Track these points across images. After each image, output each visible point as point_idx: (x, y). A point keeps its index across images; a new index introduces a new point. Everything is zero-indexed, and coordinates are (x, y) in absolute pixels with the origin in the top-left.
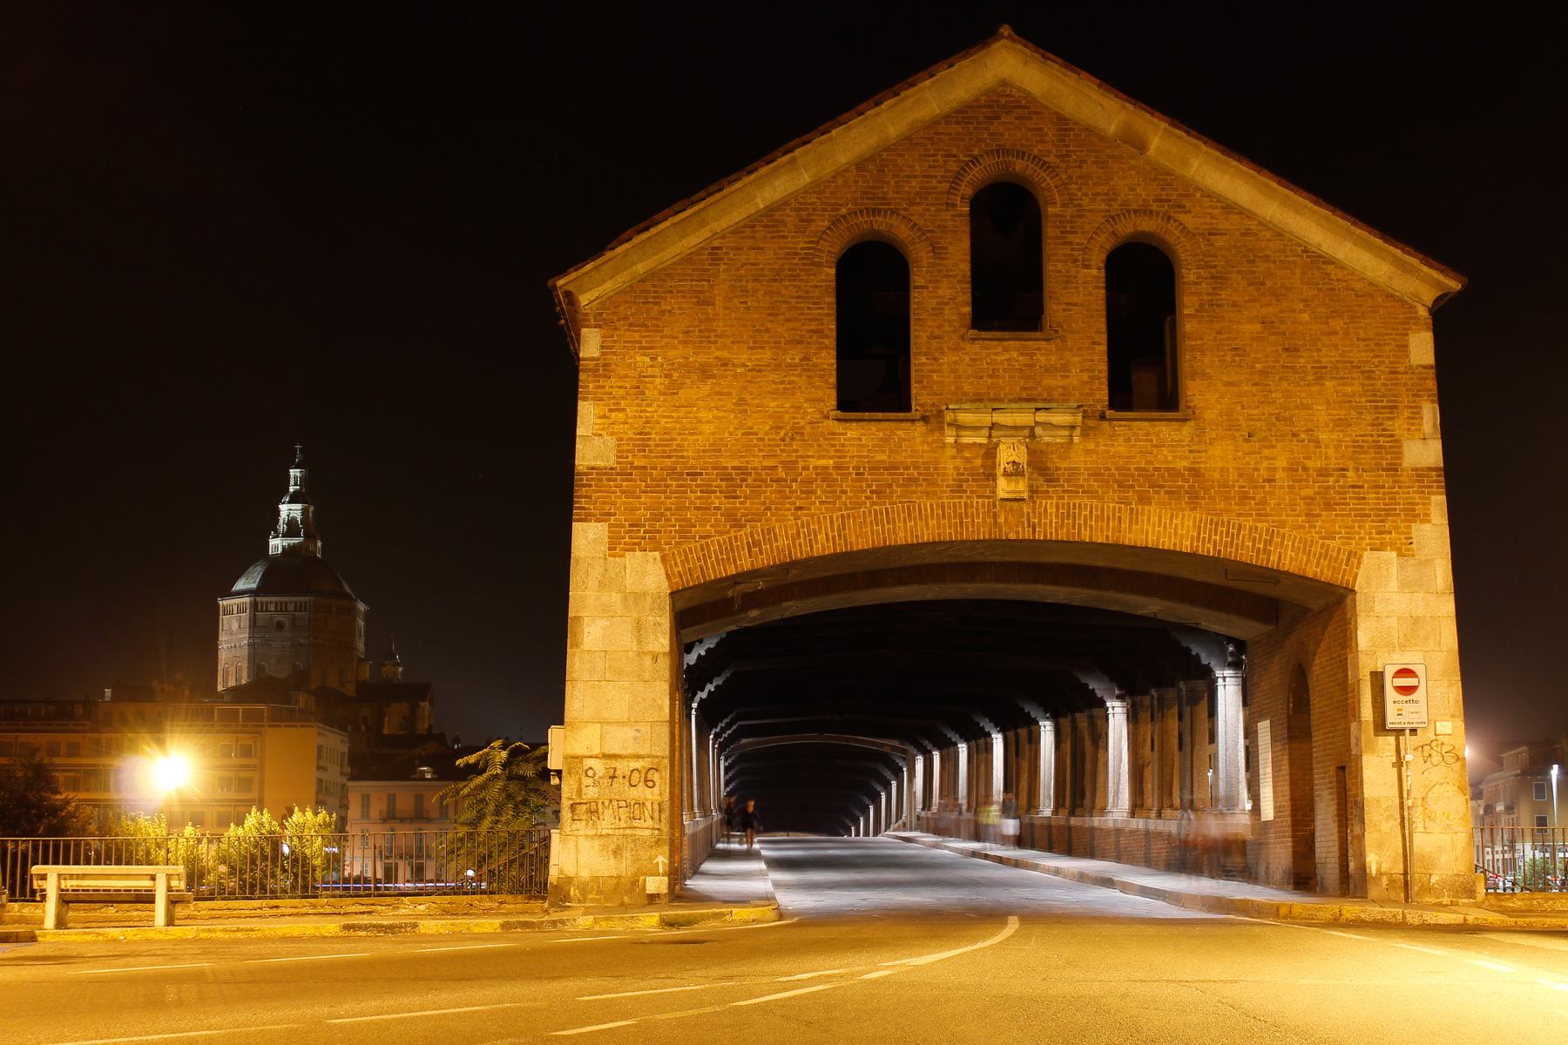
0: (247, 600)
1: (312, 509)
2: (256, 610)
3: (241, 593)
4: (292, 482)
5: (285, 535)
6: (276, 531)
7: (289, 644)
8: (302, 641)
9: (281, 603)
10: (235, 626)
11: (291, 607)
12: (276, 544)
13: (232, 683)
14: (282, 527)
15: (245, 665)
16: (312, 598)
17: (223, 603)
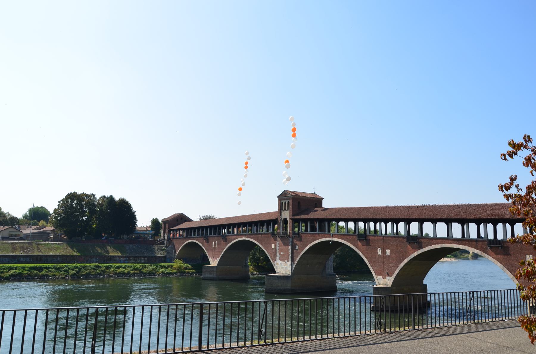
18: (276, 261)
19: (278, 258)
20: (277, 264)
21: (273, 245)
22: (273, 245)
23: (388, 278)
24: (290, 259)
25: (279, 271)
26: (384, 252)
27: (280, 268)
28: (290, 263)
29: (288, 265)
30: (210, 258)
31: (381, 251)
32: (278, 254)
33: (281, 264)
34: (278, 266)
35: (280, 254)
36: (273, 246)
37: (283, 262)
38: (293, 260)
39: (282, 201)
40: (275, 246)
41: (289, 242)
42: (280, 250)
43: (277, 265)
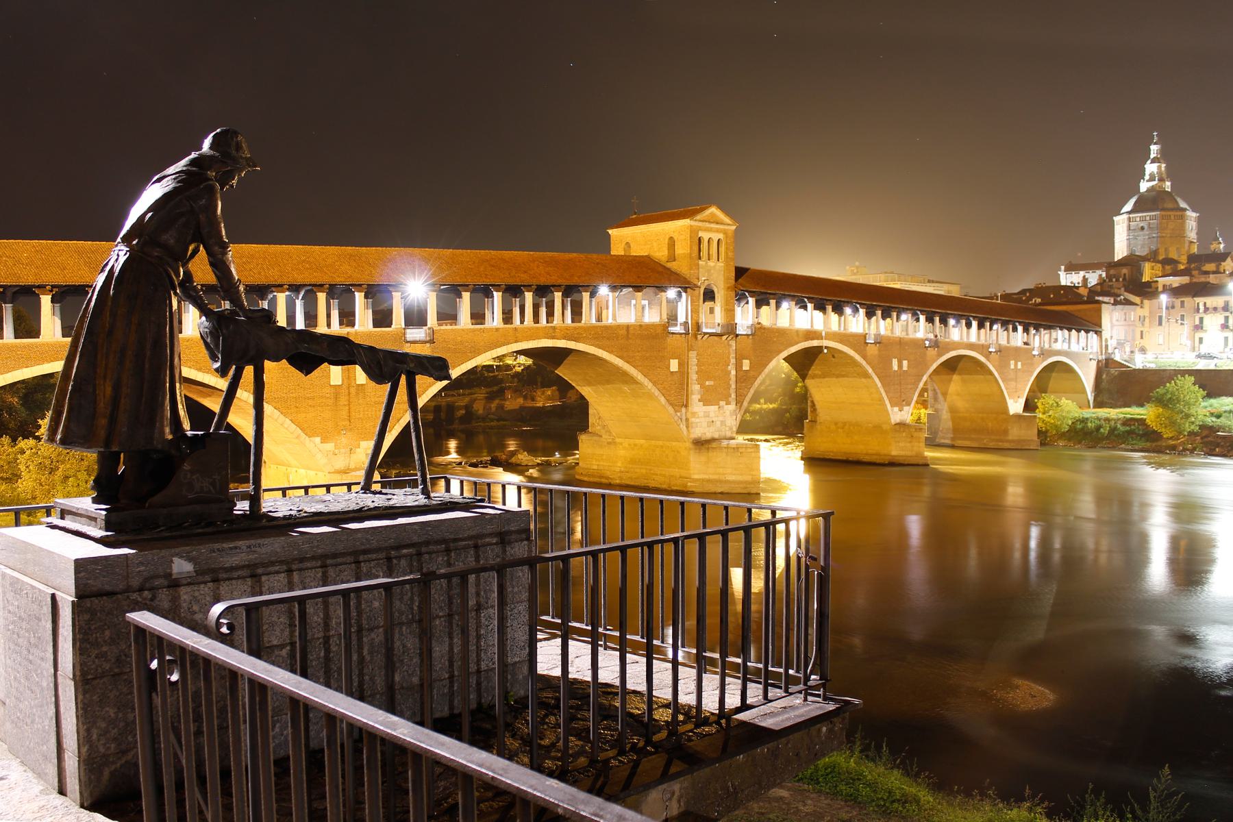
0: (1125, 216)
1: (1164, 165)
2: (1130, 222)
3: (1123, 214)
4: (1152, 152)
5: (1149, 180)
6: (1144, 180)
7: (1147, 237)
8: (1154, 235)
9: (1143, 217)
10: (1121, 229)
11: (1148, 218)
12: (1144, 186)
13: (1120, 258)
14: (1147, 177)
15: (1125, 250)
16: (1158, 213)
17: (1116, 219)
18: (686, 406)
19: (695, 398)
20: (694, 414)
21: (671, 360)
22: (671, 360)
23: (905, 408)
24: (733, 396)
25: (700, 435)
26: (900, 365)
27: (705, 424)
28: (732, 407)
29: (728, 413)
30: (318, 440)
31: (897, 362)
32: (696, 387)
33: (707, 415)
34: (697, 420)
35: (702, 386)
36: (674, 365)
37: (713, 408)
38: (739, 402)
39: (701, 234)
40: (680, 365)
41: (729, 352)
42: (703, 375)
43: (693, 419)
